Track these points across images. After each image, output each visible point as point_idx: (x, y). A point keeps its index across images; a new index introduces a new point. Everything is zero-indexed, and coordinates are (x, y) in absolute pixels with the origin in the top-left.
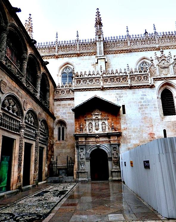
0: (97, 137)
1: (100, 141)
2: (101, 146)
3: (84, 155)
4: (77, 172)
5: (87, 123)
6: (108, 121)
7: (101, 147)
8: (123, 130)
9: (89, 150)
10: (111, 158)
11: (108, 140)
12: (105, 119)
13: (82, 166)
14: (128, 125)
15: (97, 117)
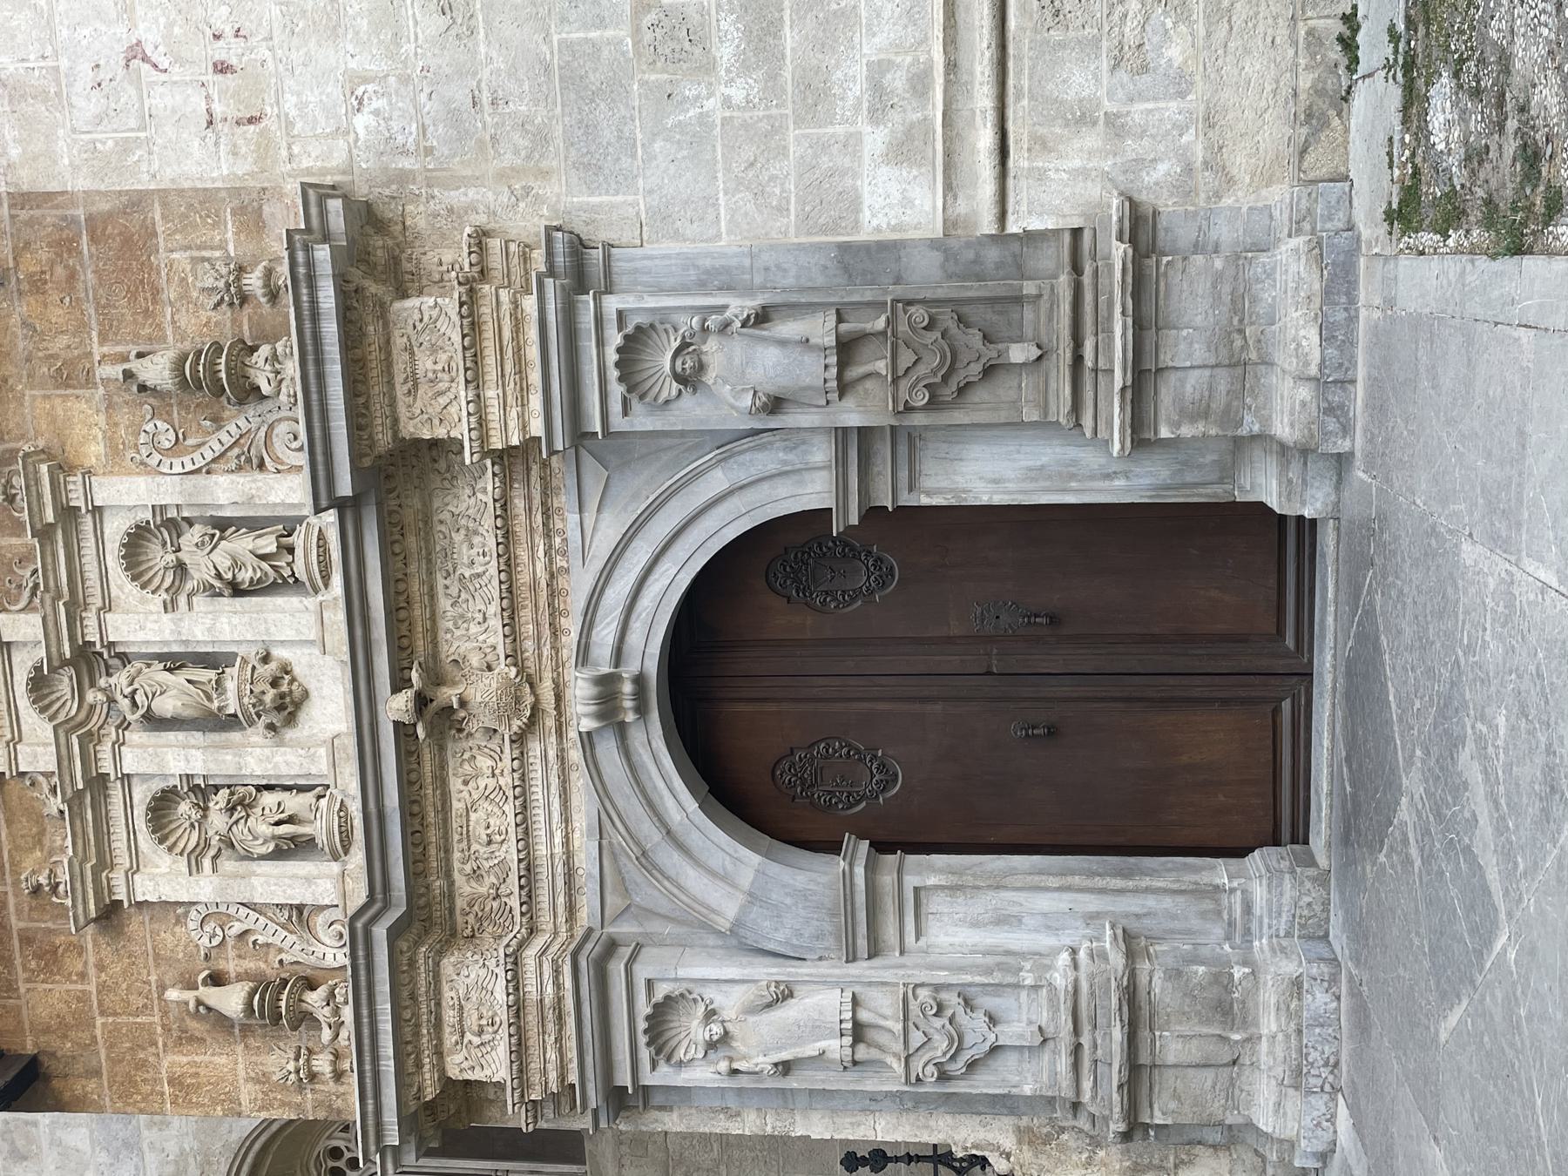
0: (422, 701)
1: (515, 657)
2: (605, 634)
3: (784, 994)
4: (1126, 1136)
5: (159, 876)
6: (94, 452)
7: (635, 638)
8: (265, 148)
9: (693, 879)
10: (857, 446)
11: (489, 484)
12: (44, 534)
13: (995, 1049)
14: (149, 34)
15: (39, 684)
